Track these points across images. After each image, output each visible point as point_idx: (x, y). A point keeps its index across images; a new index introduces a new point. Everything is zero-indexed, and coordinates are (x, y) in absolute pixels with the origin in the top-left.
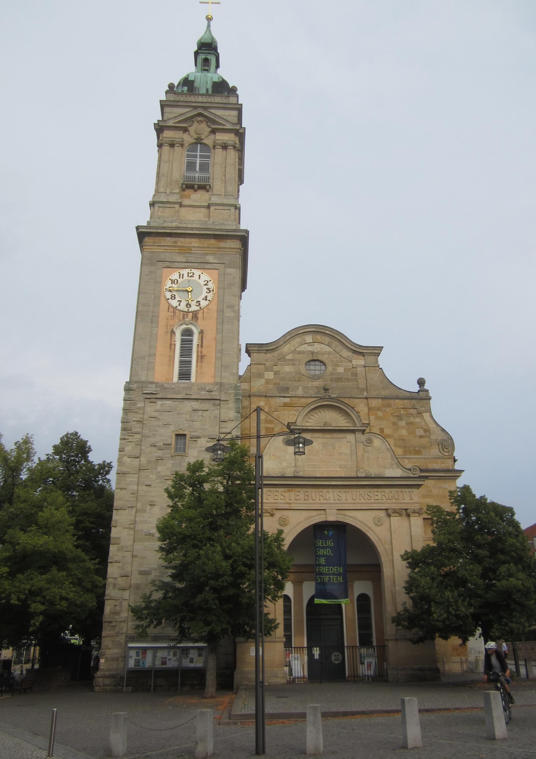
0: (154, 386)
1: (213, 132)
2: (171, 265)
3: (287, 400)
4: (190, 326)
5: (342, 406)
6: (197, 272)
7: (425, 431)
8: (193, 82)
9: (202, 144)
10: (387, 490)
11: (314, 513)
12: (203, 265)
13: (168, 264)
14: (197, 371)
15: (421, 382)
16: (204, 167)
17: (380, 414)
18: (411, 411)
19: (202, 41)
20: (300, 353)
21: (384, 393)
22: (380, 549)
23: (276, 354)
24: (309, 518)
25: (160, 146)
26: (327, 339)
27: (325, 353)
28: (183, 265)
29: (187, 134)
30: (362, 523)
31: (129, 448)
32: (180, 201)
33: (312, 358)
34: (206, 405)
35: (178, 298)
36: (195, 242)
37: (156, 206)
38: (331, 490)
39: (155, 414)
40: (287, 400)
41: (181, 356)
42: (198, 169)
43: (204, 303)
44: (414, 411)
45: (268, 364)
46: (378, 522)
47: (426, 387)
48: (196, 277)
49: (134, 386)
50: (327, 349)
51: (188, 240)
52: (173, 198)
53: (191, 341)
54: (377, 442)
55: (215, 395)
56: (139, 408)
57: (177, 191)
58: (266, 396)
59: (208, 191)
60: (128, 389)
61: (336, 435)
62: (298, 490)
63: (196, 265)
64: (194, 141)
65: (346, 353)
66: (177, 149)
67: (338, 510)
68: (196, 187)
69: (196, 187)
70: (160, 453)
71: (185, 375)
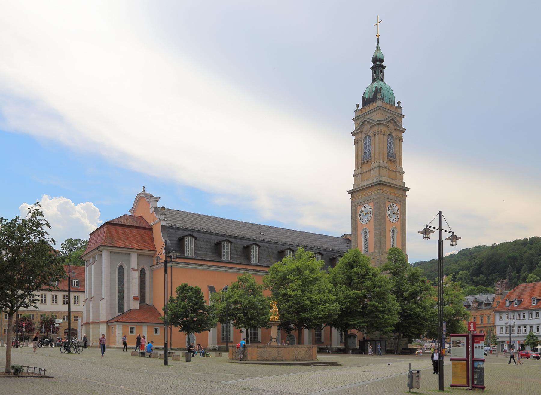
6: (367, 205)
43: (370, 219)
52: (359, 171)
66: (360, 144)
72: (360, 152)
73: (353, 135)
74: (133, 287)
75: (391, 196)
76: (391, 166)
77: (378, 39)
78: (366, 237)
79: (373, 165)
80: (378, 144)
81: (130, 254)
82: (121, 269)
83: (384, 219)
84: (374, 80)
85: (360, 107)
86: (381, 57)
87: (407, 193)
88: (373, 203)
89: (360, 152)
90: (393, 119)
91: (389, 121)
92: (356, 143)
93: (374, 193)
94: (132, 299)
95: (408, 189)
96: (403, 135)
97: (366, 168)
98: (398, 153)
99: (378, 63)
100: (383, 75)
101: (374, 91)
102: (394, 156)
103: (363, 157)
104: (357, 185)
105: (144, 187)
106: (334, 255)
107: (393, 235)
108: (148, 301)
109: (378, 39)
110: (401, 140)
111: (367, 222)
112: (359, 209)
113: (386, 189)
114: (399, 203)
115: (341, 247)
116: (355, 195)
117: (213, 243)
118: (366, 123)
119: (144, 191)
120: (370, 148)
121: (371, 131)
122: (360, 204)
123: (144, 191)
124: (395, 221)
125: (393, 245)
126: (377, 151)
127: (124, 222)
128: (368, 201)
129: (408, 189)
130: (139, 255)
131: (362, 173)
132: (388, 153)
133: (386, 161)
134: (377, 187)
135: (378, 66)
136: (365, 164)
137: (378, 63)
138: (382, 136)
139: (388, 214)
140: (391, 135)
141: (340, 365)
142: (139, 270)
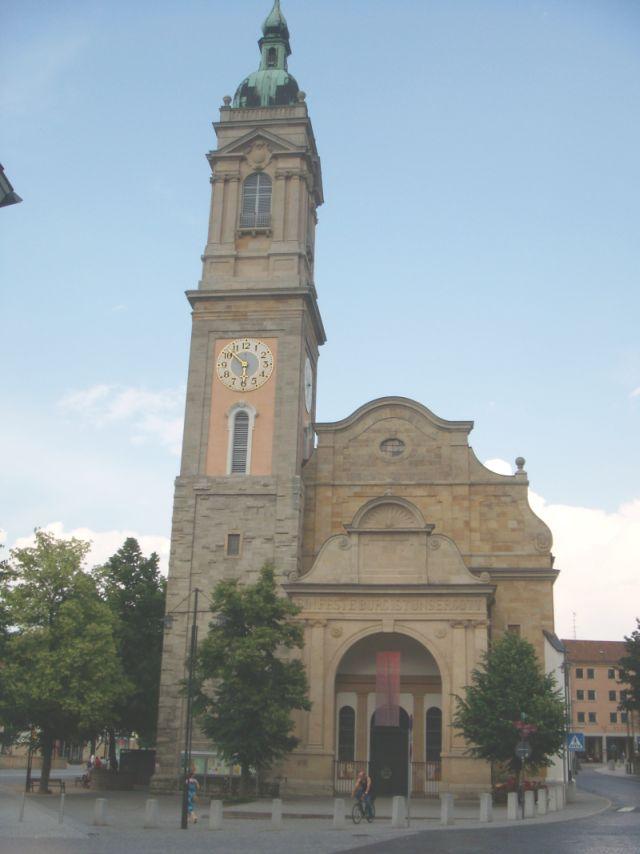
0: (205, 480)
1: (275, 157)
2: (226, 335)
3: (357, 489)
4: (246, 410)
5: (406, 506)
6: (253, 342)
7: (519, 522)
8: (254, 88)
9: (262, 174)
10: (452, 599)
11: (369, 624)
12: (260, 333)
13: (221, 334)
14: (251, 463)
15: (520, 463)
16: (265, 205)
17: (466, 503)
18: (503, 499)
19: (268, 25)
20: (374, 431)
21: (474, 479)
22: (440, 662)
23: (347, 435)
24: (364, 629)
25: (213, 181)
26: (407, 414)
27: (407, 431)
28: (237, 334)
29: (243, 164)
30: (422, 635)
31: (179, 551)
32: (235, 253)
33: (388, 436)
34: (259, 503)
35: (232, 375)
36: (252, 306)
37: (209, 261)
38: (389, 600)
39: (207, 513)
40: (357, 489)
41: (236, 443)
42: (257, 211)
44: (508, 499)
45: (337, 446)
46: (442, 636)
47: (525, 468)
48: (252, 350)
49: (184, 481)
50: (408, 425)
51: (243, 303)
53: (247, 425)
54: (444, 545)
55: (271, 489)
56: (190, 507)
57: (232, 240)
58: (333, 485)
59: (268, 237)
60: (179, 485)
61: (397, 537)
62: (353, 598)
63: (252, 333)
64: (253, 172)
65: (430, 430)
66: (233, 185)
67: (396, 620)
68: (254, 233)
69: (254, 233)
70: (210, 557)
71: (238, 466)
88: (275, 341)
118: (258, 142)
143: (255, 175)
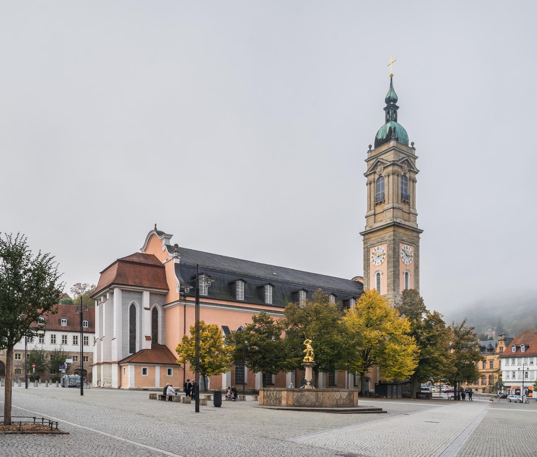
6: (380, 247)
43: (383, 260)
52: (372, 212)
66: (372, 185)
72: (372, 194)
73: (366, 176)
74: (145, 327)
75: (405, 238)
76: (405, 207)
77: (391, 79)
78: (378, 279)
79: (386, 206)
80: (390, 186)
81: (142, 293)
82: (133, 309)
83: (398, 261)
84: (387, 121)
85: (373, 148)
86: (395, 97)
87: (421, 235)
89: (372, 194)
90: (407, 160)
91: (403, 162)
92: (369, 184)
93: (389, 234)
94: (144, 339)
95: (421, 231)
96: (417, 176)
97: (379, 209)
98: (411, 195)
99: (392, 103)
100: (396, 116)
101: (388, 131)
102: (408, 197)
103: (376, 199)
104: (370, 227)
105: (156, 225)
106: (347, 297)
107: (407, 277)
108: (160, 342)
109: (391, 79)
110: (414, 181)
111: (380, 264)
112: (372, 250)
113: (401, 230)
114: (413, 245)
115: (354, 289)
116: (367, 237)
117: (226, 282)
118: (379, 163)
119: (156, 229)
120: (383, 189)
121: (385, 172)
122: (373, 245)
123: (156, 229)
124: (408, 264)
125: (407, 287)
126: (391, 192)
127: (135, 259)
128: (380, 243)
129: (421, 231)
130: (151, 294)
131: (375, 215)
132: (402, 194)
133: (400, 202)
134: (391, 229)
135: (391, 106)
136: (378, 206)
137: (392, 103)
138: (396, 177)
139: (401, 256)
140: (404, 175)
141: (386, 412)
142: (151, 309)
143: (379, 178)
